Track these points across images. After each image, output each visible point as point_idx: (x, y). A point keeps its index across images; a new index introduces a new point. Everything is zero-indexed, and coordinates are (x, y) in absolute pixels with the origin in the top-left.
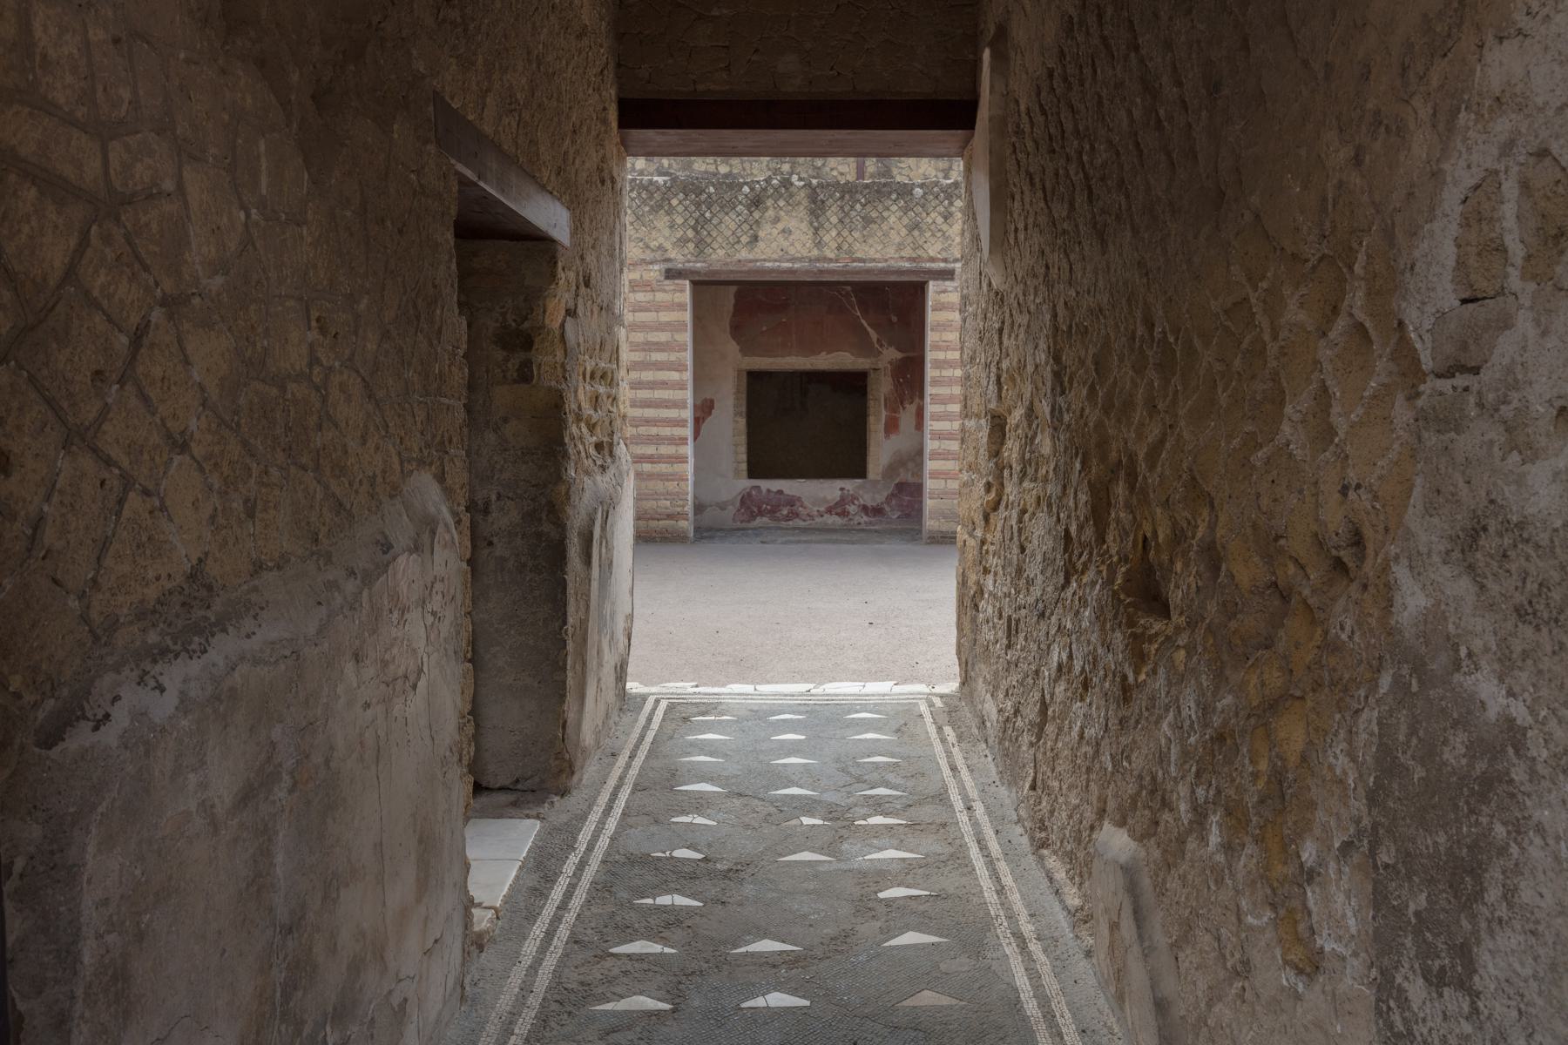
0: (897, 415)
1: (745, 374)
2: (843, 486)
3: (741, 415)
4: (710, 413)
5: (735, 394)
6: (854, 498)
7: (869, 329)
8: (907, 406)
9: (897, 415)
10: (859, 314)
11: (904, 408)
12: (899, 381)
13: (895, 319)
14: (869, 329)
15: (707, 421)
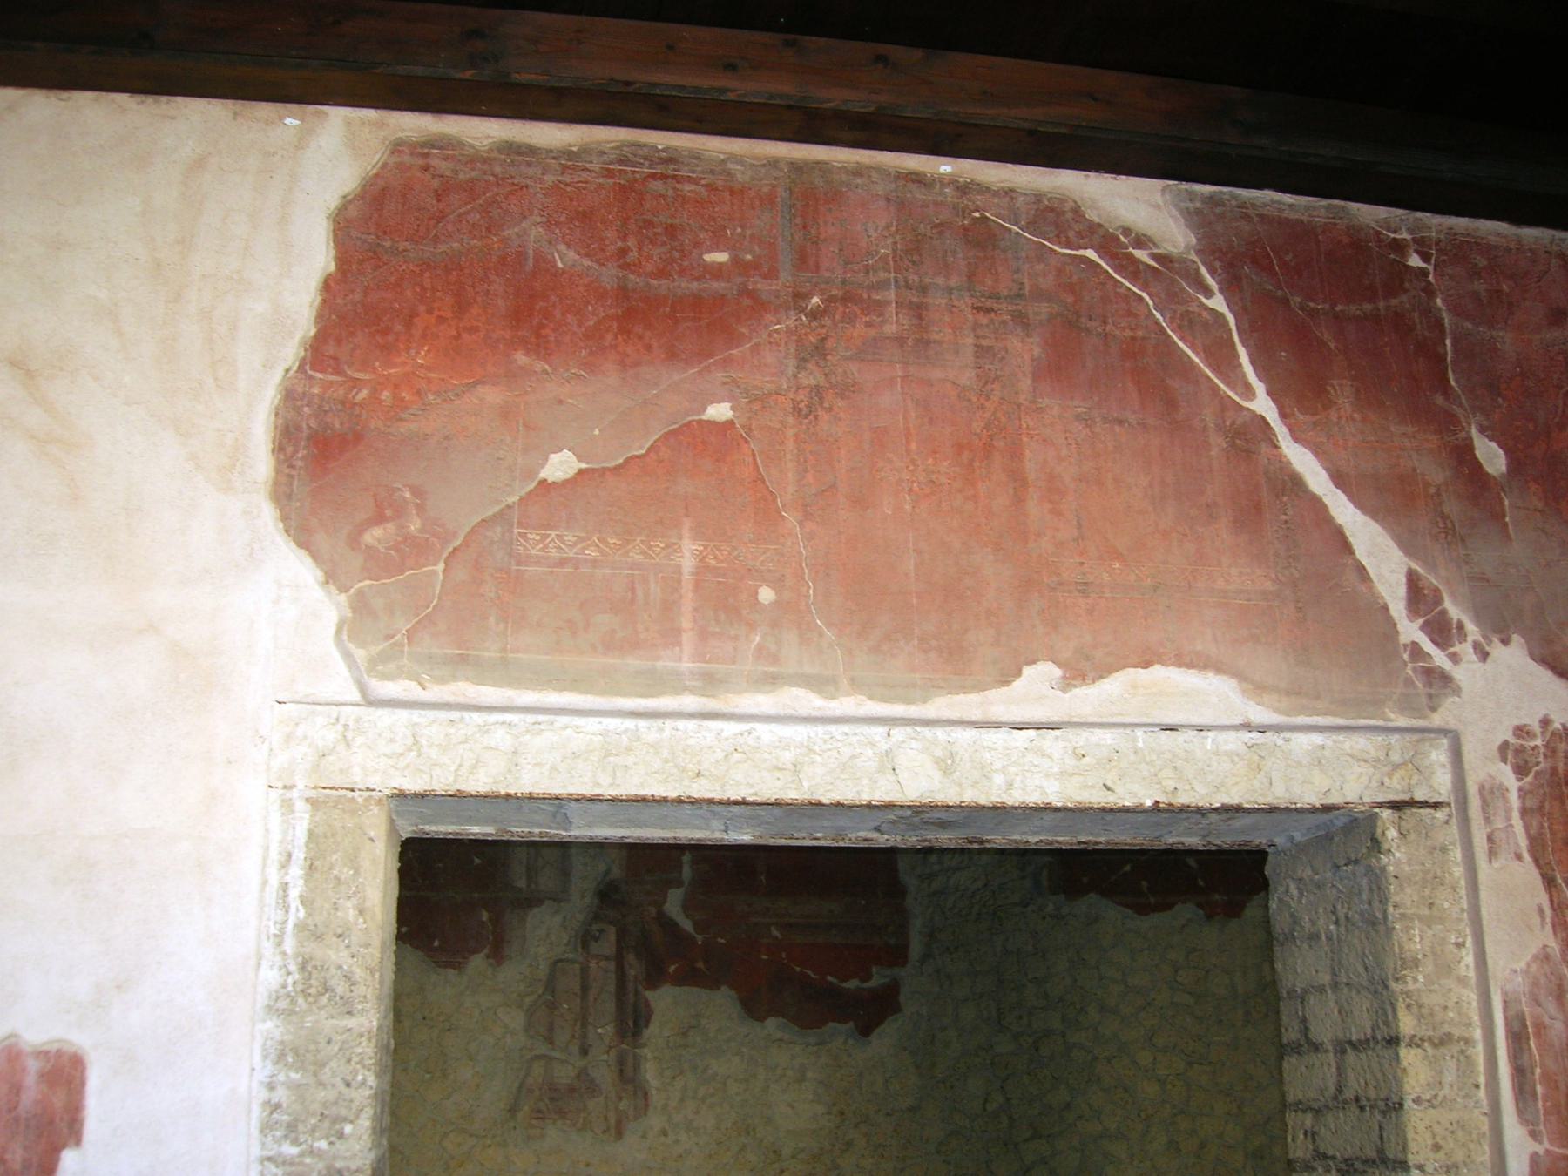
5: (282, 1006)
7: (1343, 511)
10: (1263, 405)
13: (1492, 457)
14: (1343, 511)
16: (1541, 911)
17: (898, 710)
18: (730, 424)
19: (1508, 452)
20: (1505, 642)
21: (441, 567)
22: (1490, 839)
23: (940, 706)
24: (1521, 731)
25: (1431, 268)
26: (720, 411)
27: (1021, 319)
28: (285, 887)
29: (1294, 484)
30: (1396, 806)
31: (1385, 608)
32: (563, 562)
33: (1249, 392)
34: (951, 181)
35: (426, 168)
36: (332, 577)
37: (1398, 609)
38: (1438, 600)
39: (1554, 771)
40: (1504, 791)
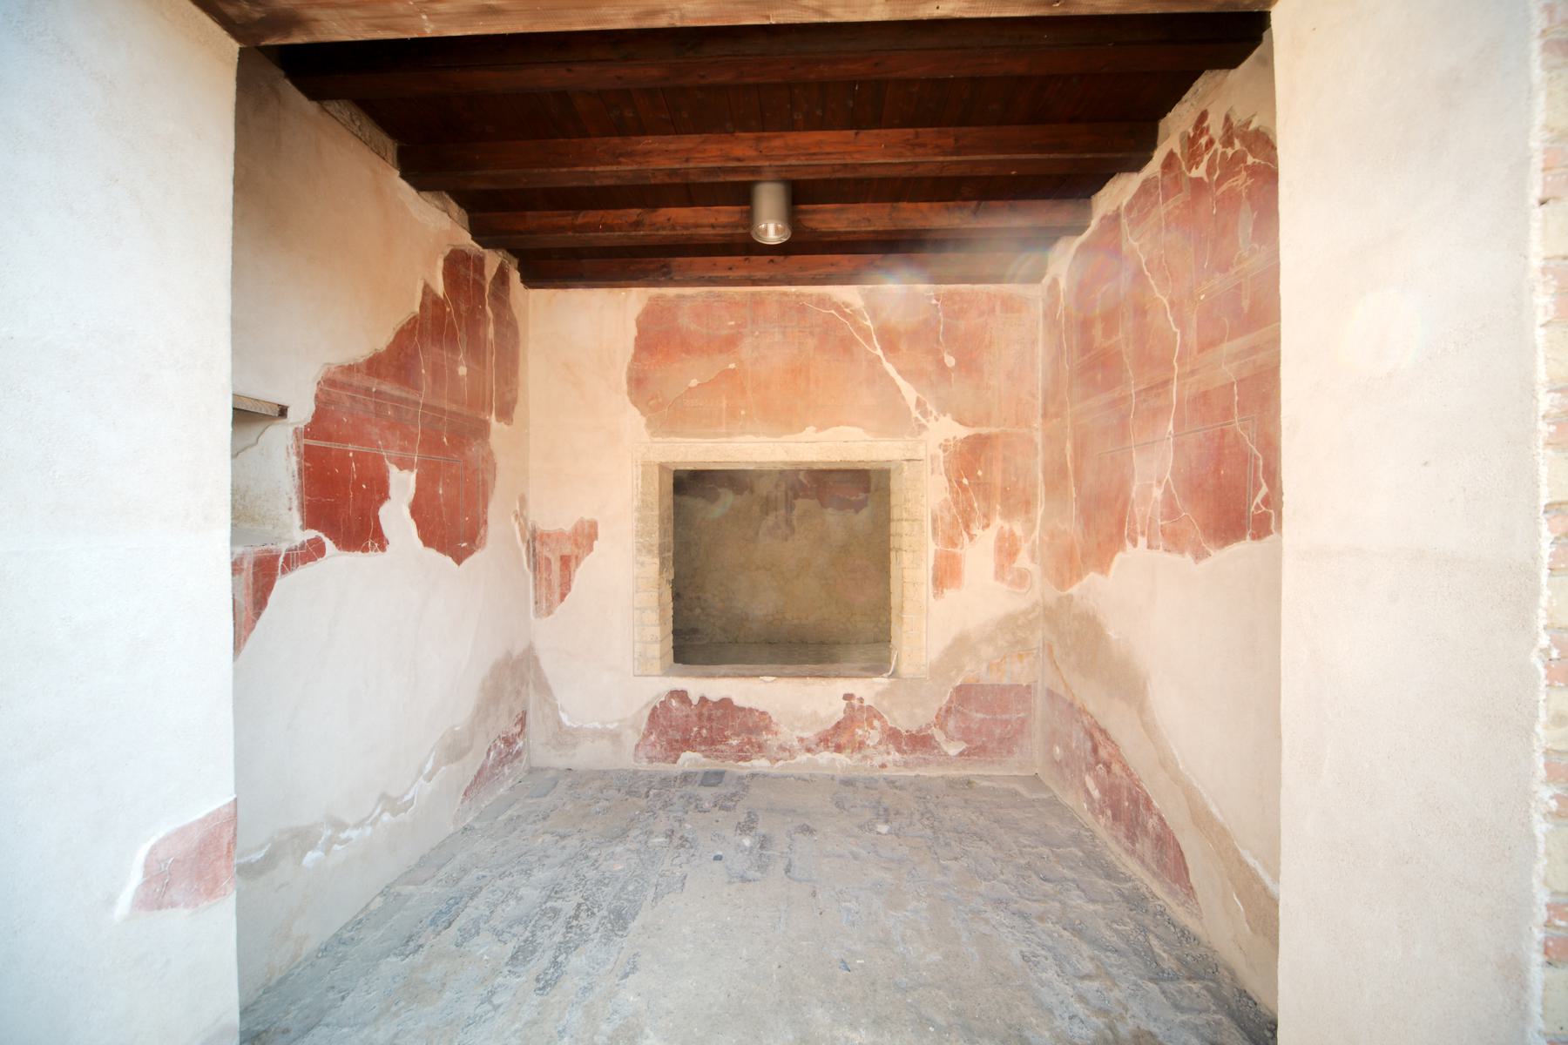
0: (957, 550)
1: (656, 470)
2: (850, 691)
3: (649, 552)
4: (591, 549)
5: (638, 510)
6: (873, 714)
7: (900, 381)
8: (976, 530)
9: (957, 550)
10: (879, 352)
11: (972, 537)
12: (960, 483)
13: (950, 361)
14: (900, 381)
15: (582, 565)
16: (946, 488)
17: (774, 440)
18: (734, 369)
19: (956, 359)
20: (945, 416)
21: (666, 410)
22: (932, 469)
23: (784, 438)
24: (946, 440)
25: (939, 303)
26: (732, 366)
27: (812, 333)
28: (637, 485)
29: (887, 374)
30: (908, 460)
31: (909, 408)
32: (694, 407)
33: (875, 348)
34: (794, 294)
35: (658, 304)
36: (643, 413)
37: (913, 408)
38: (925, 405)
39: (955, 451)
40: (939, 457)
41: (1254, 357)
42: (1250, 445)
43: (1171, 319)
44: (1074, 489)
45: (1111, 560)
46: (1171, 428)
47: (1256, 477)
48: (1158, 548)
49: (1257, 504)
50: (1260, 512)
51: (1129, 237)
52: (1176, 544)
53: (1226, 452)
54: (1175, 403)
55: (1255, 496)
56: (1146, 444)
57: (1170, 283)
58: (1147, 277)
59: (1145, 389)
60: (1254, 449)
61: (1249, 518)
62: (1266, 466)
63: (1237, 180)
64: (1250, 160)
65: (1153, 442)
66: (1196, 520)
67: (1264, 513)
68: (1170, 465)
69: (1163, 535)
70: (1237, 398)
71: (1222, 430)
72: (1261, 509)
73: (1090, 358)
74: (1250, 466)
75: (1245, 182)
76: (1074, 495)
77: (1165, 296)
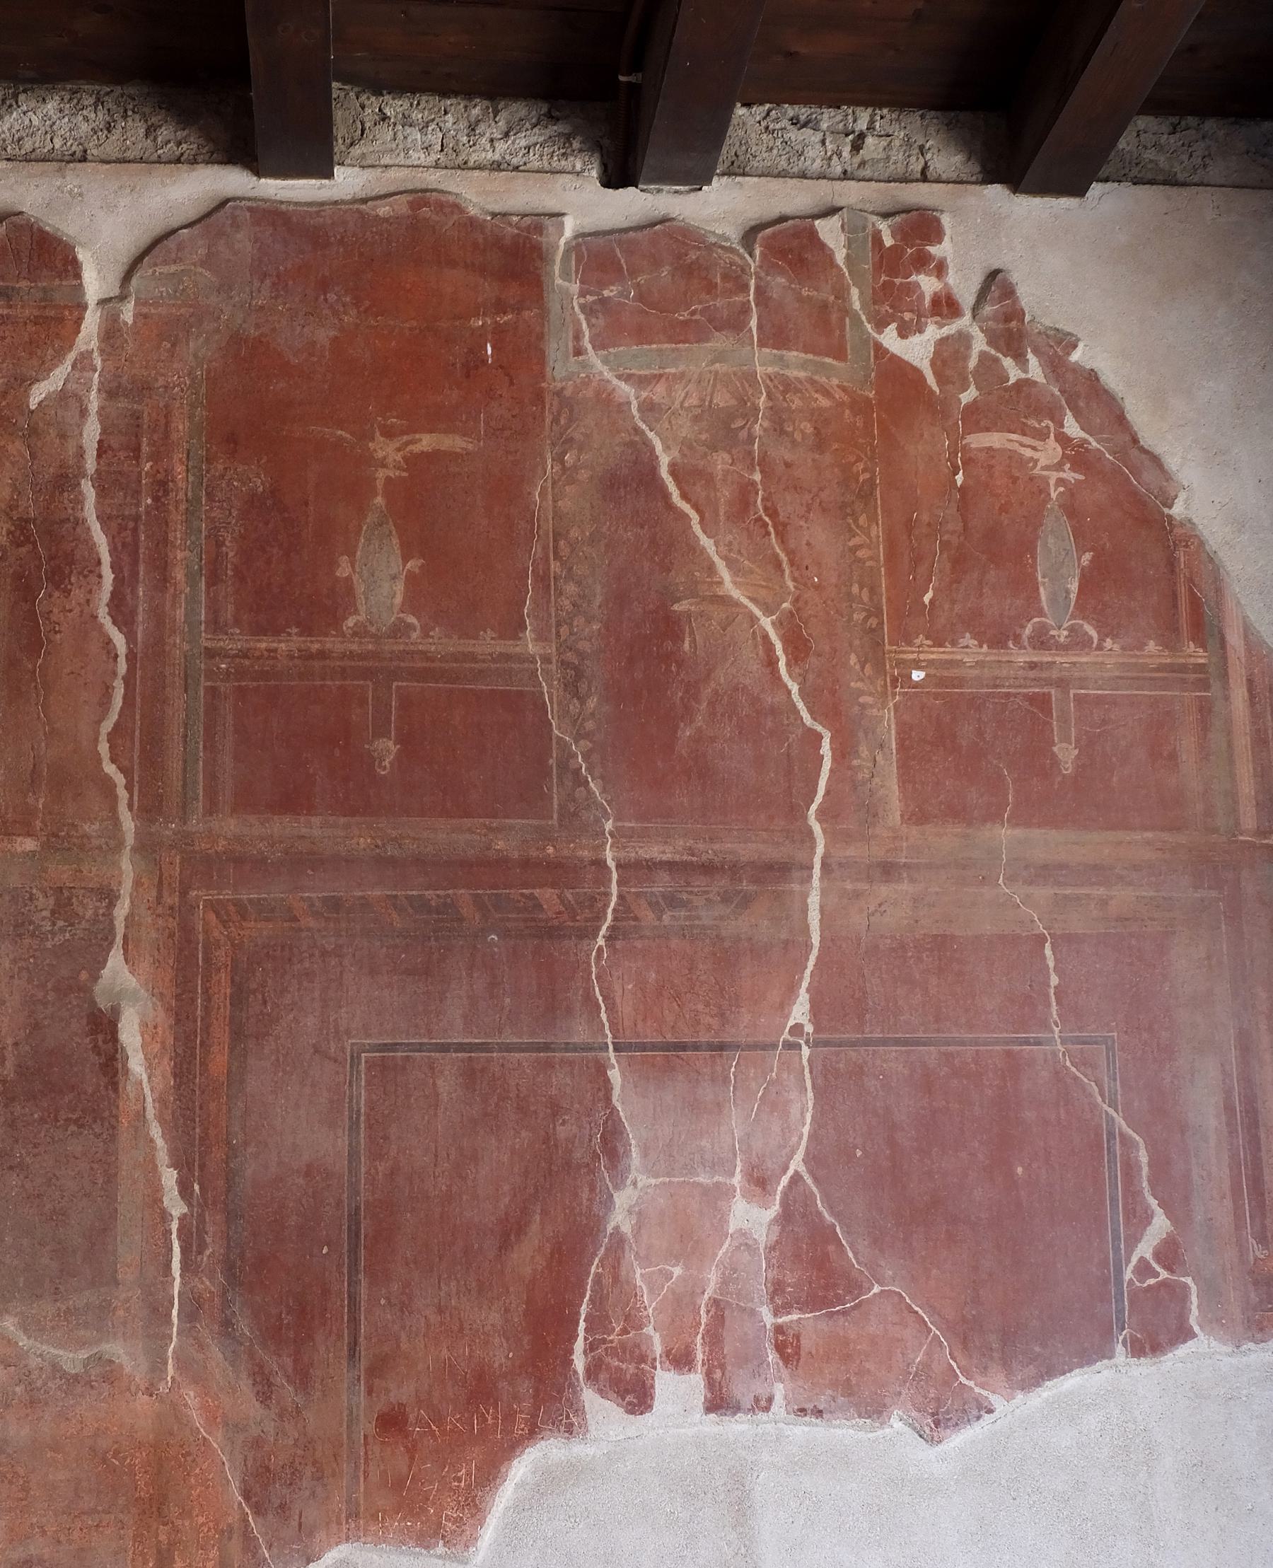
41: (1101, 891)
42: (1105, 1107)
43: (794, 688)
44: (169, 1178)
45: (490, 1474)
46: (800, 1012)
47: (1132, 1193)
48: (763, 1404)
49: (1142, 1259)
50: (1152, 1281)
51: (586, 343)
52: (848, 1389)
53: (1029, 1115)
54: (816, 940)
55: (1133, 1240)
56: (683, 1047)
57: (790, 584)
58: (684, 517)
59: (671, 866)
60: (1120, 1121)
61: (1120, 1300)
62: (1160, 1165)
63: (1034, 448)
64: (1072, 428)
65: (721, 1047)
66: (932, 1310)
67: (1164, 1284)
68: (806, 1130)
69: (786, 1359)
70: (1054, 980)
71: (1009, 1054)
72: (1156, 1275)
73: (308, 656)
74: (1112, 1161)
75: (1059, 467)
76: (176, 1207)
77: (768, 611)
